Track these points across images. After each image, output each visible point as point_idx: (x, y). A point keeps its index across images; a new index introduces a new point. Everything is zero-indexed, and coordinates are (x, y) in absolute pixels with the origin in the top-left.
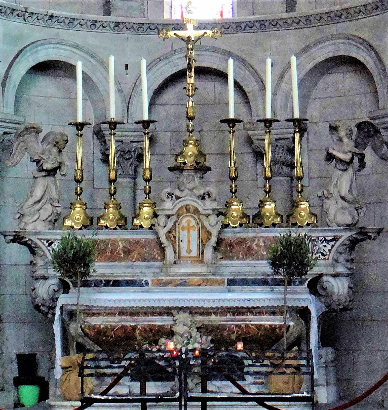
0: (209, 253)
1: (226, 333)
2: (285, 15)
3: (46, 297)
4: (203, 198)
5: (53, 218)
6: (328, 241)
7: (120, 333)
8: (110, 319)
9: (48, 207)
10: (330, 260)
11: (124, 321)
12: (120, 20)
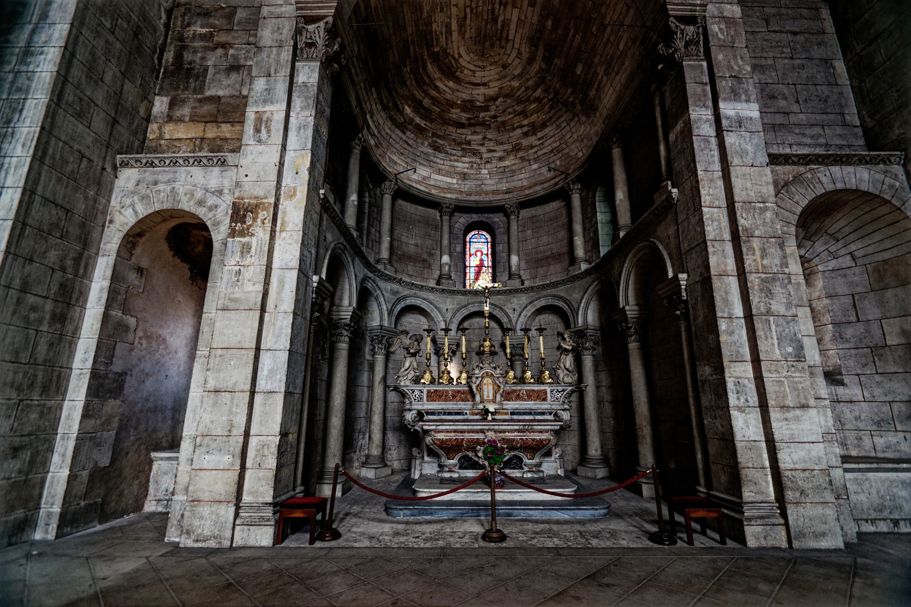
0: (498, 397)
1: (514, 443)
2: (521, 287)
3: (410, 420)
4: (495, 368)
5: (414, 378)
6: (560, 392)
7: (454, 443)
8: (449, 434)
9: (412, 372)
12: (444, 288)
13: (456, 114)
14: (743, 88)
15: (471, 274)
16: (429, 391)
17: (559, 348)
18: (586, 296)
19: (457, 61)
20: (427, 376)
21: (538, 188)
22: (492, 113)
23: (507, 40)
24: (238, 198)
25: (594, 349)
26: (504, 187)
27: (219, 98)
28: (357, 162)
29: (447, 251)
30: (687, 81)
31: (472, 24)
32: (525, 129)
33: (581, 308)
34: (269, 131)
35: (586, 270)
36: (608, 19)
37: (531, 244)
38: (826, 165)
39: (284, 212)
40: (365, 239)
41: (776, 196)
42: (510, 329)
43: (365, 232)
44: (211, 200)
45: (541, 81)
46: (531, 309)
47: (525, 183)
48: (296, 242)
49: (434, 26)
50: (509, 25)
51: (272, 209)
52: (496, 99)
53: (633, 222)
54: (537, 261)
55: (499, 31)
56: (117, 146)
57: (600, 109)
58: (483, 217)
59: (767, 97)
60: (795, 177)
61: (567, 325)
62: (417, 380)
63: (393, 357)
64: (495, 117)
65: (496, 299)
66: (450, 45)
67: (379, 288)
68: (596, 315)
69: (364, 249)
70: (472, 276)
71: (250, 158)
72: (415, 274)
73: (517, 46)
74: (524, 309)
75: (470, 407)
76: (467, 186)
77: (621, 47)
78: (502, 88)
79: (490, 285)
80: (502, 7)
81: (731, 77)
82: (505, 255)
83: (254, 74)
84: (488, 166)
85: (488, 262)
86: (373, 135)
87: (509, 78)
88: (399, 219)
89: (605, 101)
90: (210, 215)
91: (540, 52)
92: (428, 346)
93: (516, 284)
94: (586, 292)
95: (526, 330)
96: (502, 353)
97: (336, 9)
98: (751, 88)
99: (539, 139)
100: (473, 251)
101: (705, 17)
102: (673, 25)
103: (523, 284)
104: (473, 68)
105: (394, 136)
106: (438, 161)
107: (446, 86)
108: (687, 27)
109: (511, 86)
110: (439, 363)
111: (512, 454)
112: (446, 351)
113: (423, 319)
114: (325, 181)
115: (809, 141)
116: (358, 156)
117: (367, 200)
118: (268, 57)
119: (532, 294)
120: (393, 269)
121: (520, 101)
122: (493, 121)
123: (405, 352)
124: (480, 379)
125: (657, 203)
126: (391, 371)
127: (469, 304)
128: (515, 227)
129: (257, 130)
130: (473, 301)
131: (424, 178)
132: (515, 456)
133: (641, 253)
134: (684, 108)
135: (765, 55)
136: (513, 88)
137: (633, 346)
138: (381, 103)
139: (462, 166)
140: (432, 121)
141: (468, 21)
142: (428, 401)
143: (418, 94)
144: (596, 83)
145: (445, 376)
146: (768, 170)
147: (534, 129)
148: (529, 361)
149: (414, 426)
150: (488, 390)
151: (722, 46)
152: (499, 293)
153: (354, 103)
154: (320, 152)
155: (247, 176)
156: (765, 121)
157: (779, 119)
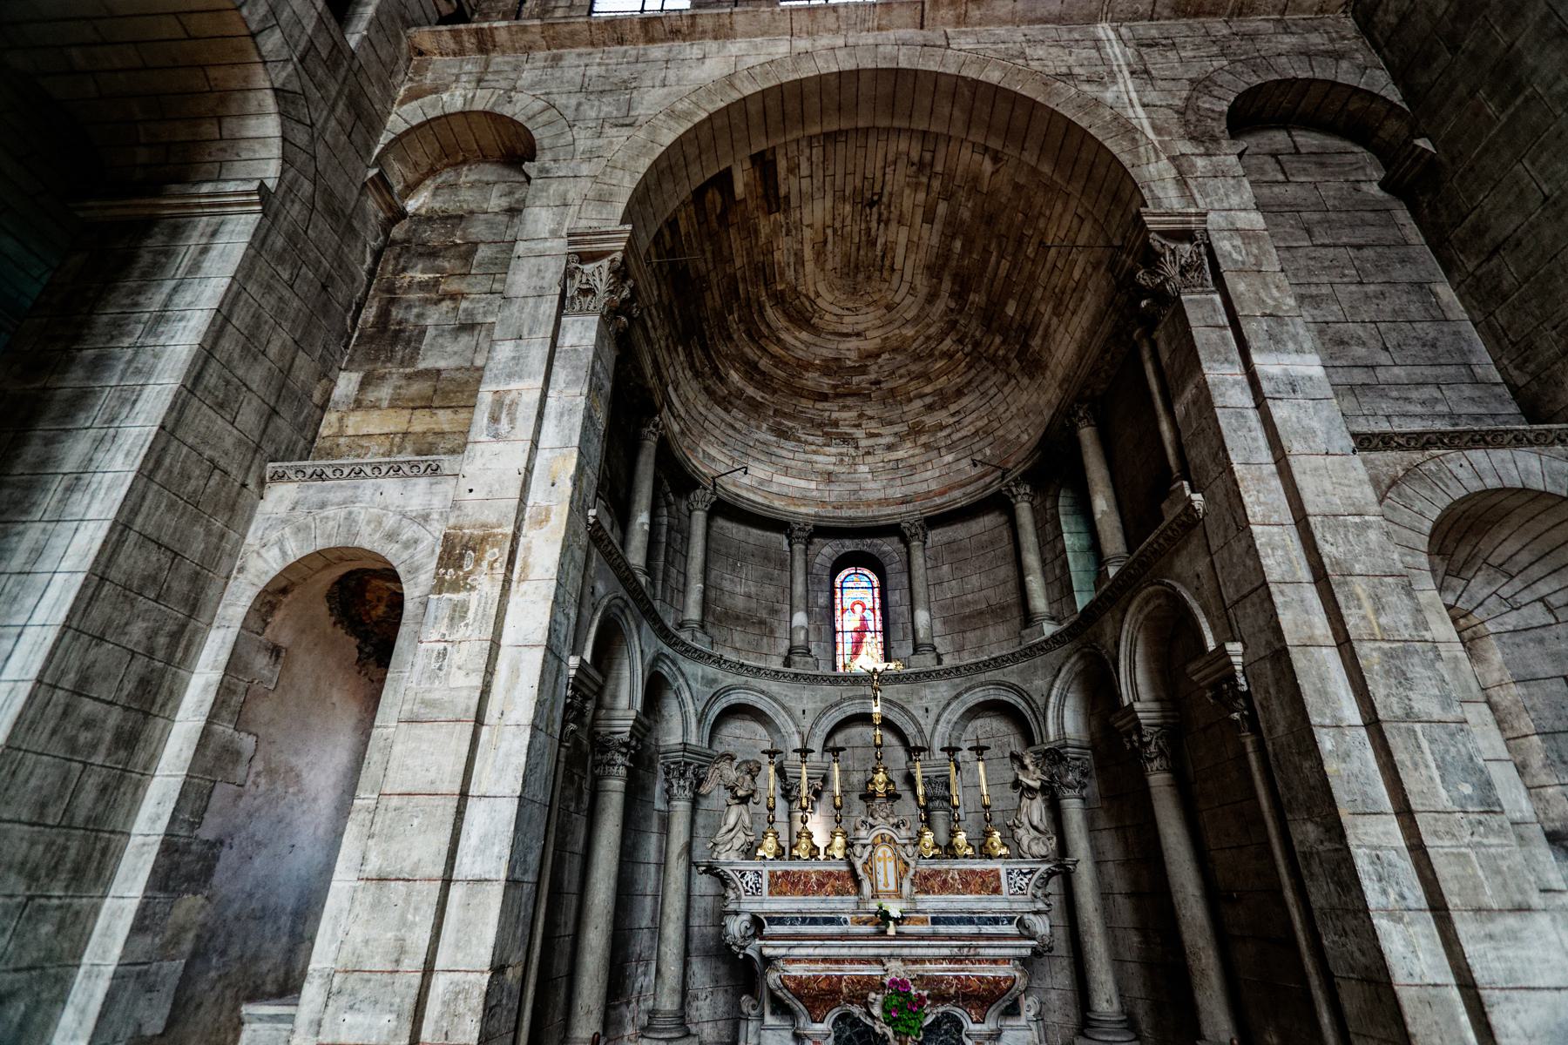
1: (943, 987)
2: (937, 668)
3: (737, 935)
4: (898, 827)
5: (745, 848)
6: (1025, 874)
7: (824, 985)
8: (813, 966)
9: (741, 835)
10: (1029, 896)
11: (828, 970)
13: (811, 379)
14: (1287, 332)
15: (845, 644)
16: (772, 874)
17: (1016, 784)
18: (1058, 684)
19: (813, 302)
20: (770, 843)
21: (957, 494)
22: (873, 377)
23: (893, 270)
24: (454, 528)
25: (1084, 786)
26: (897, 492)
27: (439, 371)
28: (652, 460)
29: (802, 606)
30: (1192, 323)
31: (836, 250)
32: (928, 400)
33: (1051, 706)
34: (512, 421)
35: (1053, 636)
36: (1051, 237)
37: (951, 589)
38: (1459, 448)
39: (528, 549)
40: (659, 587)
41: (1380, 502)
42: (922, 749)
43: (660, 576)
44: (409, 532)
45: (953, 325)
46: (957, 709)
47: (934, 486)
48: (545, 598)
49: (777, 255)
50: (893, 249)
51: (508, 544)
52: (878, 356)
53: (1130, 550)
54: (963, 619)
55: (879, 259)
56: (269, 449)
57: (1052, 367)
58: (864, 545)
59: (1333, 343)
60: (1407, 470)
61: (1028, 740)
62: (750, 852)
63: (705, 804)
64: (877, 382)
65: (890, 691)
66: (801, 280)
67: (683, 674)
68: (1081, 720)
69: (657, 604)
70: (848, 648)
71: (478, 463)
72: (746, 647)
73: (908, 277)
74: (945, 709)
75: (852, 906)
76: (836, 492)
77: (1076, 275)
78: (887, 338)
79: (881, 666)
80: (882, 225)
81: (1264, 315)
82: (905, 609)
83: (496, 336)
84: (869, 459)
85: (874, 622)
86: (677, 417)
87: (897, 324)
88: (717, 551)
89: (1059, 354)
90: (405, 556)
91: (946, 285)
92: (769, 781)
93: (926, 662)
94: (1056, 676)
95: (951, 750)
96: (907, 795)
97: (629, 241)
98: (1301, 332)
99: (953, 415)
100: (847, 605)
101: (1206, 230)
102: (1156, 243)
103: (940, 661)
104: (840, 311)
105: (711, 417)
106: (784, 453)
107: (796, 340)
108: (1180, 246)
109: (901, 334)
110: (790, 815)
111: (941, 1009)
112: (804, 792)
113: (760, 730)
114: (597, 495)
115: (1419, 409)
116: (653, 451)
117: (665, 520)
118: (521, 310)
119: (957, 681)
120: (707, 639)
121: (917, 358)
122: (874, 388)
123: (729, 794)
124: (870, 848)
125: (1169, 518)
126: (701, 832)
127: (843, 700)
128: (921, 561)
129: (494, 419)
130: (851, 694)
131: (762, 482)
132: (946, 1015)
133: (1151, 606)
134: (1191, 362)
135: (1315, 280)
136: (904, 339)
137: (1158, 780)
138: (692, 366)
139: (826, 459)
140: (774, 392)
141: (830, 247)
142: (771, 893)
143: (751, 352)
144: (1041, 328)
145: (804, 843)
146: (1357, 460)
147: (943, 400)
148: (961, 811)
149: (743, 948)
150: (886, 872)
151: (1241, 271)
152: (897, 678)
153: (649, 371)
154: (592, 450)
155: (471, 491)
156: (1337, 381)
157: (1359, 376)
